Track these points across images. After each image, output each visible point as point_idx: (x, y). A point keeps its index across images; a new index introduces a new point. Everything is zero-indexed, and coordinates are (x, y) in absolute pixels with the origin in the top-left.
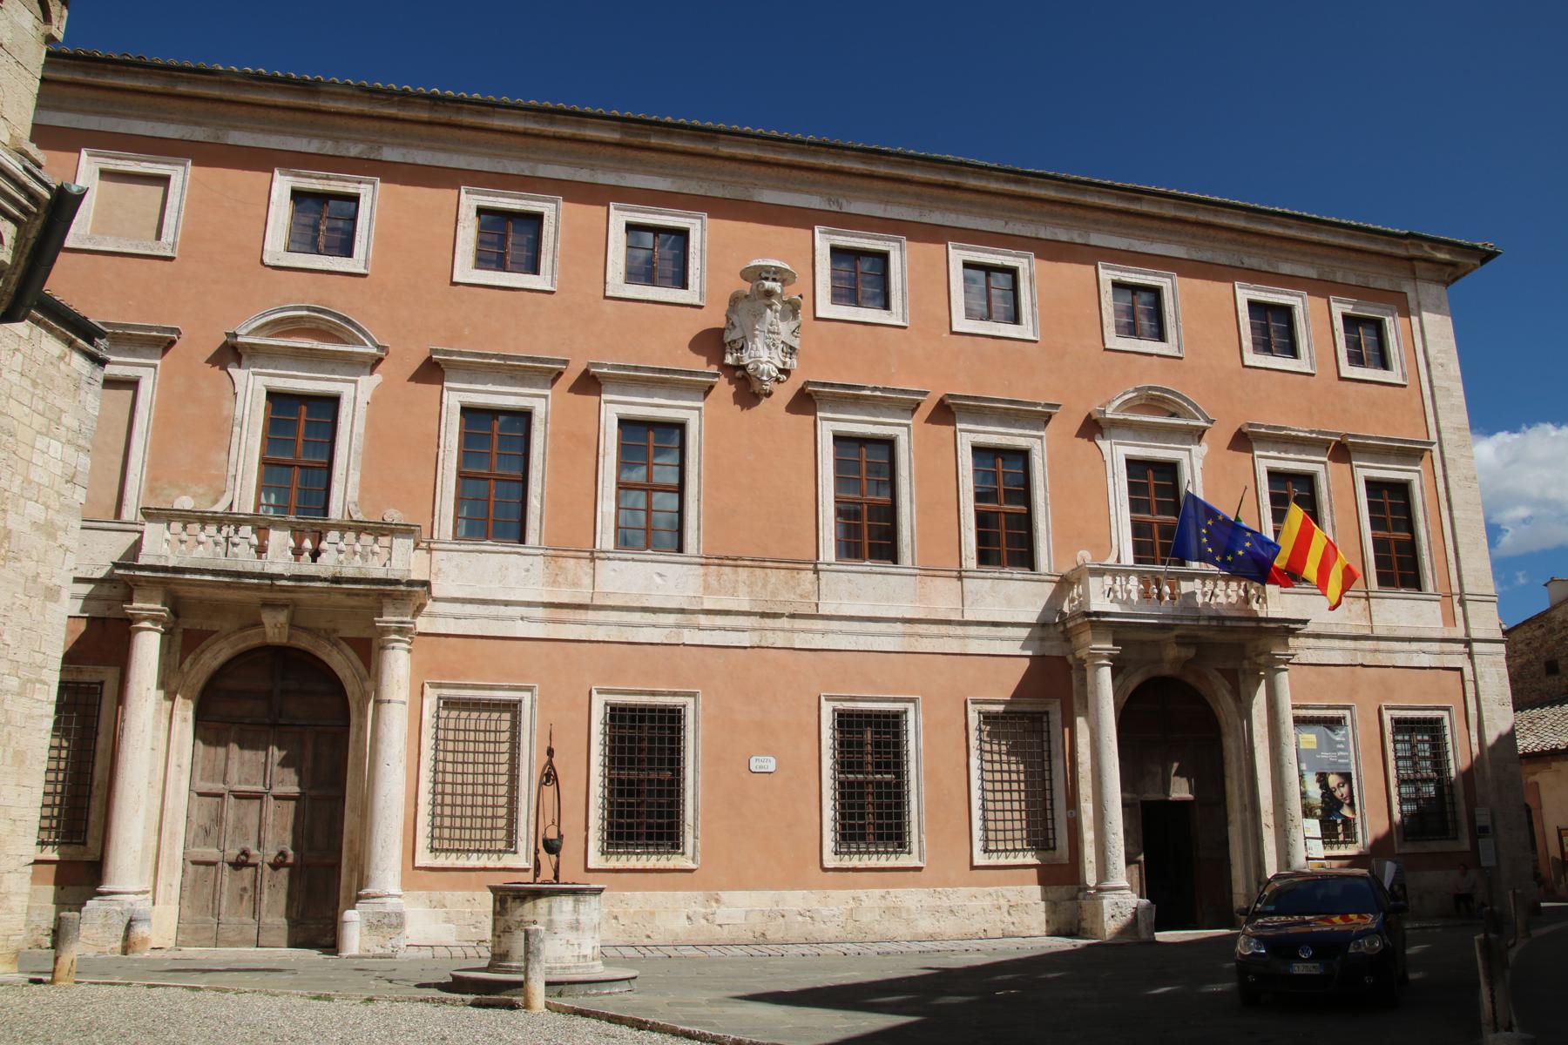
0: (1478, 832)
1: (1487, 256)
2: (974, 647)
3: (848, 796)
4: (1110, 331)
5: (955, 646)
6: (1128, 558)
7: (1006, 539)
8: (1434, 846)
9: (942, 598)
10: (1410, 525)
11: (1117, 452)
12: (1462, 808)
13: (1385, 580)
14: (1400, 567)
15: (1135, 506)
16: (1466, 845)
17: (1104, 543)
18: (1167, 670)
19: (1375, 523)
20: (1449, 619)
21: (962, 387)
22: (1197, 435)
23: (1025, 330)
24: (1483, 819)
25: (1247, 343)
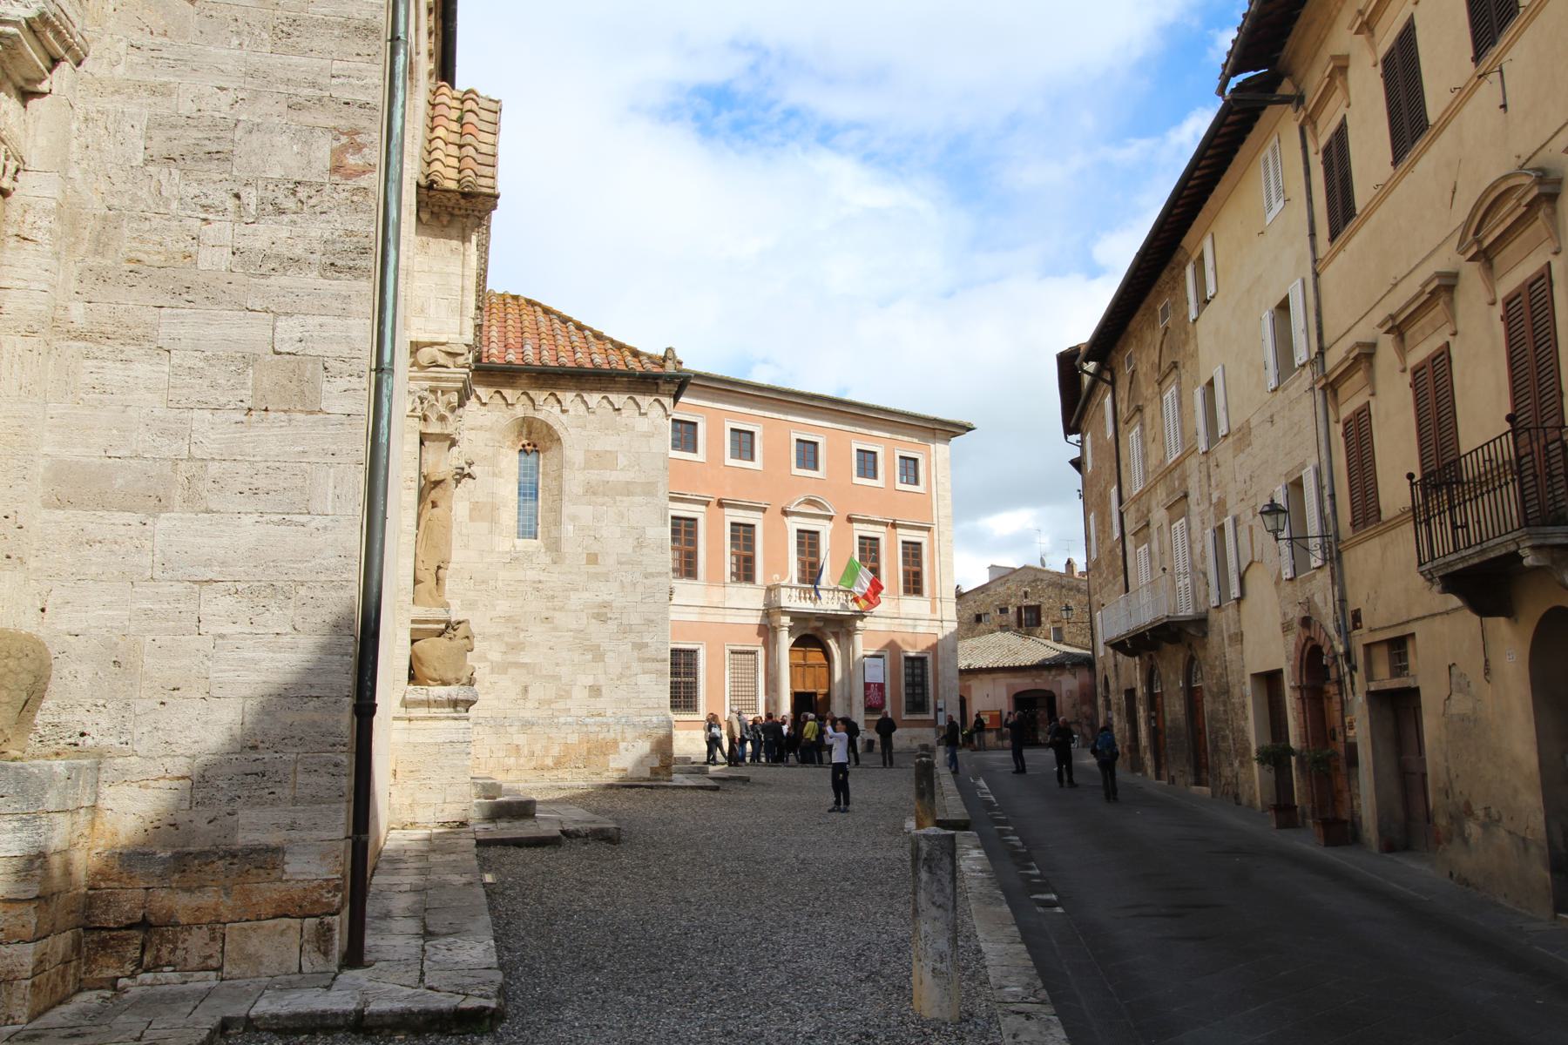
0: (937, 710)
1: (969, 429)
2: (729, 620)
3: (675, 687)
4: (794, 464)
5: (720, 619)
6: (795, 582)
7: (745, 571)
8: (918, 717)
9: (716, 595)
10: (919, 564)
11: (794, 524)
12: (931, 700)
13: (907, 591)
14: (914, 584)
15: (800, 552)
16: (931, 717)
17: (784, 574)
18: (809, 632)
19: (905, 562)
20: (933, 610)
21: (727, 496)
22: (830, 518)
23: (757, 465)
24: (940, 706)
25: (855, 472)
